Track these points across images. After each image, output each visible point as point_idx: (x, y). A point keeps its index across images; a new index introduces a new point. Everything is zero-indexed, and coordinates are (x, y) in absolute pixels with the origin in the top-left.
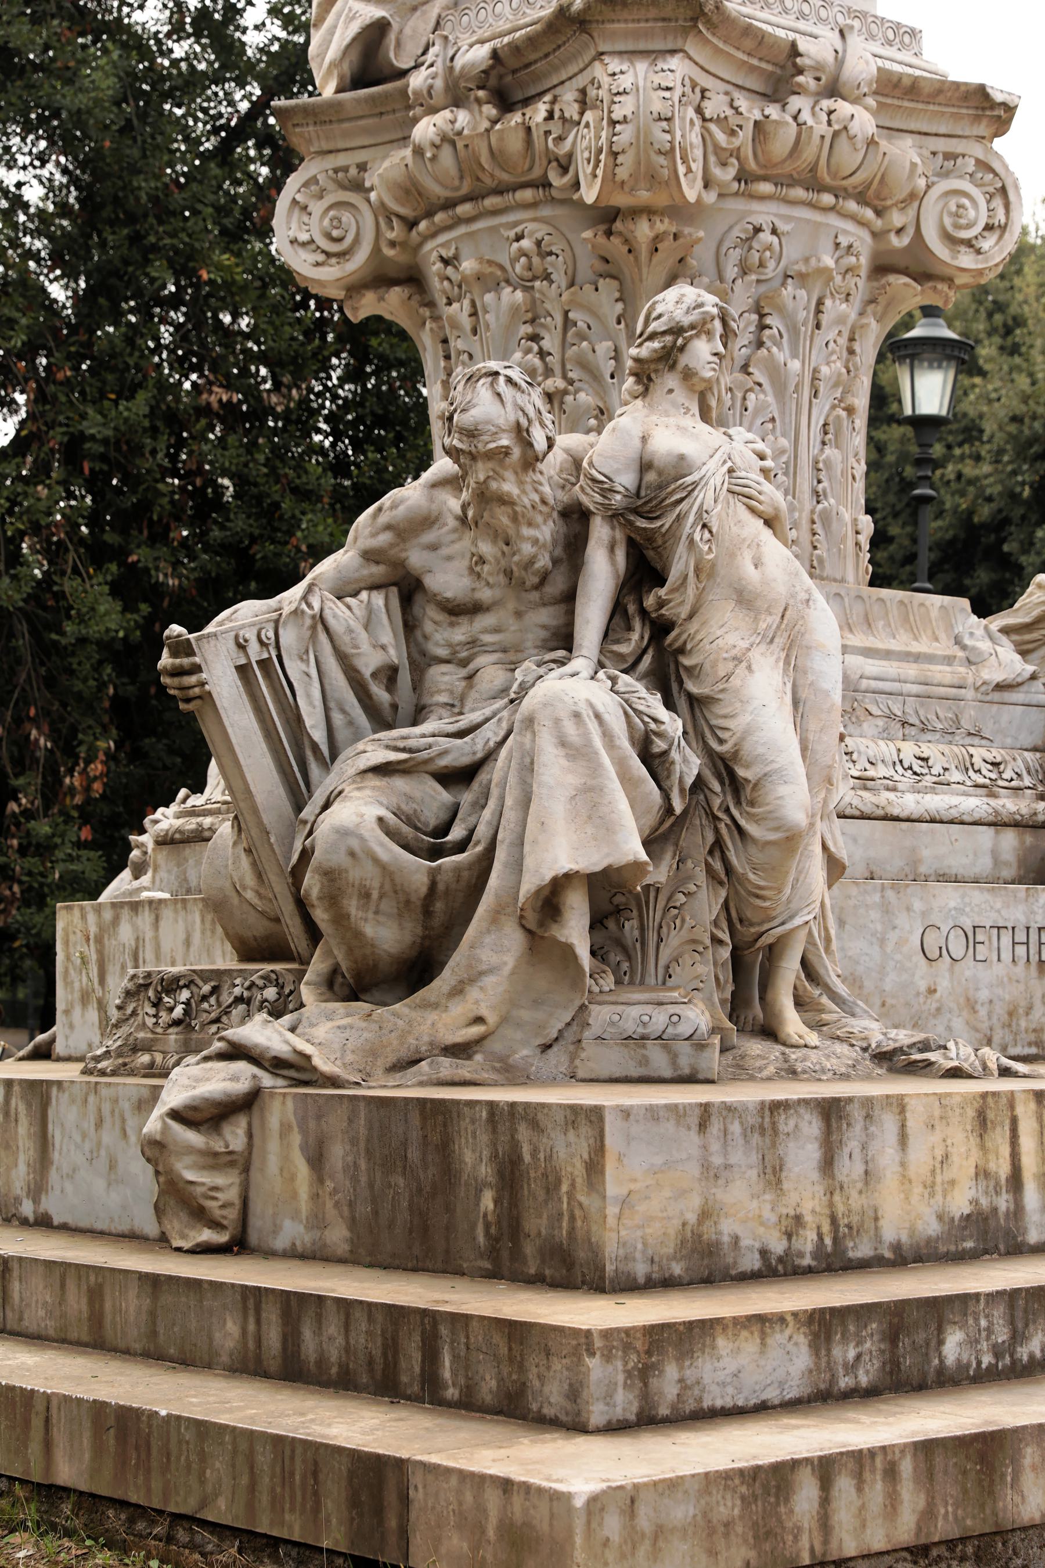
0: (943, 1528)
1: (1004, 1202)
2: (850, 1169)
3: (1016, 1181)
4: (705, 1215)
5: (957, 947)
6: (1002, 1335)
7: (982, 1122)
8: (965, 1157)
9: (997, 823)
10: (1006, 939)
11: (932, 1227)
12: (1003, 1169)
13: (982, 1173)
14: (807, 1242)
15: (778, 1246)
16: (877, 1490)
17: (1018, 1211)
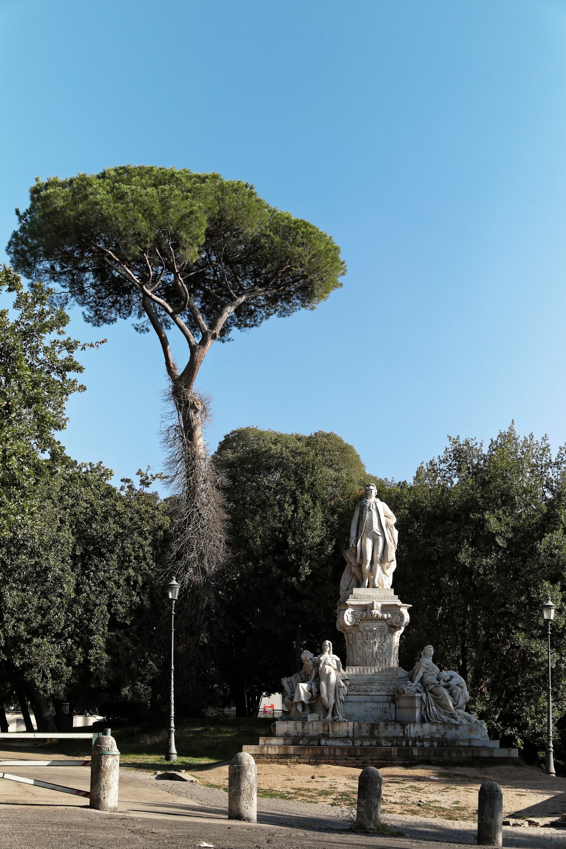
0: (281, 753)
1: (327, 733)
2: (306, 728)
3: (328, 731)
4: (287, 731)
5: (371, 710)
6: (307, 742)
7: (324, 725)
8: (321, 727)
9: (388, 695)
10: (379, 709)
11: (317, 734)
12: (327, 729)
13: (323, 730)
14: (300, 735)
15: (296, 735)
16: (273, 749)
17: (329, 734)
